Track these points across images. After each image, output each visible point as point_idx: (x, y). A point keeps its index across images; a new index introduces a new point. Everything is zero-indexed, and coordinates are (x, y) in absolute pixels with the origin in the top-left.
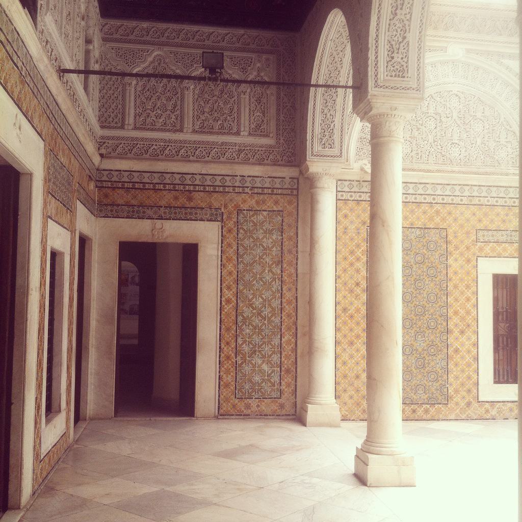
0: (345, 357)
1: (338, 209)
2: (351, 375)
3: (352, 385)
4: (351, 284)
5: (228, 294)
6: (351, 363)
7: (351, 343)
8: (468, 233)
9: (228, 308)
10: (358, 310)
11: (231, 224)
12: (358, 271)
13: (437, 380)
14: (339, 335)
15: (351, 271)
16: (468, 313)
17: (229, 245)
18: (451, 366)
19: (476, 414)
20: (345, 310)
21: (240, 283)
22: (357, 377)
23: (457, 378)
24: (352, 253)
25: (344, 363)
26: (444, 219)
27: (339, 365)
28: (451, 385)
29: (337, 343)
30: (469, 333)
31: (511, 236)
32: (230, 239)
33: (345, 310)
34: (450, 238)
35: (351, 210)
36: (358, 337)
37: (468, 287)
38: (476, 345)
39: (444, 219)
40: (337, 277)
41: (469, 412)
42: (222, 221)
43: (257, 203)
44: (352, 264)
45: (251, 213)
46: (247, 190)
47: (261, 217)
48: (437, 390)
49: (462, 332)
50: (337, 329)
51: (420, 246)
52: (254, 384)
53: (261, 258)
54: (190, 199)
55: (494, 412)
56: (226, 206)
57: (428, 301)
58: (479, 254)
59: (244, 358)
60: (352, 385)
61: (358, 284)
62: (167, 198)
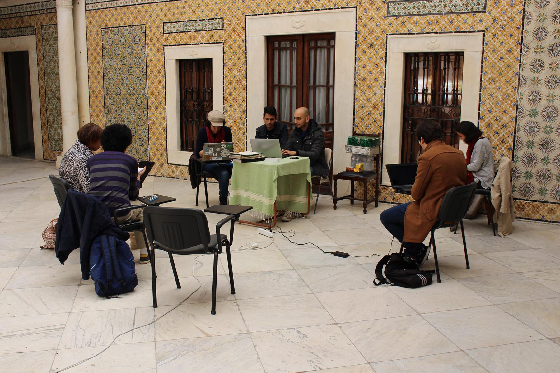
1: (86, 18)
5: (42, 84)
7: (97, 116)
8: (158, 26)
9: (42, 91)
10: (100, 92)
11: (39, 37)
12: (98, 63)
13: (142, 146)
14: (92, 110)
16: (160, 93)
17: (40, 50)
18: (151, 135)
19: (166, 173)
20: (93, 92)
21: (46, 75)
23: (154, 144)
24: (95, 49)
26: (143, 17)
28: (151, 149)
30: (161, 109)
31: (186, 26)
33: (93, 92)
34: (148, 32)
37: (159, 71)
38: (165, 119)
39: (143, 17)
40: (89, 68)
41: (163, 171)
42: (36, 34)
43: (49, 19)
44: (95, 58)
45: (47, 27)
46: (45, 11)
47: (51, 29)
48: (143, 152)
49: (156, 108)
50: (90, 106)
51: (130, 40)
52: (56, 141)
53: (53, 58)
54: (23, 22)
55: (178, 173)
56: (37, 24)
57: (136, 84)
58: (165, 44)
59: (50, 125)
61: (99, 73)
62: (14, 23)
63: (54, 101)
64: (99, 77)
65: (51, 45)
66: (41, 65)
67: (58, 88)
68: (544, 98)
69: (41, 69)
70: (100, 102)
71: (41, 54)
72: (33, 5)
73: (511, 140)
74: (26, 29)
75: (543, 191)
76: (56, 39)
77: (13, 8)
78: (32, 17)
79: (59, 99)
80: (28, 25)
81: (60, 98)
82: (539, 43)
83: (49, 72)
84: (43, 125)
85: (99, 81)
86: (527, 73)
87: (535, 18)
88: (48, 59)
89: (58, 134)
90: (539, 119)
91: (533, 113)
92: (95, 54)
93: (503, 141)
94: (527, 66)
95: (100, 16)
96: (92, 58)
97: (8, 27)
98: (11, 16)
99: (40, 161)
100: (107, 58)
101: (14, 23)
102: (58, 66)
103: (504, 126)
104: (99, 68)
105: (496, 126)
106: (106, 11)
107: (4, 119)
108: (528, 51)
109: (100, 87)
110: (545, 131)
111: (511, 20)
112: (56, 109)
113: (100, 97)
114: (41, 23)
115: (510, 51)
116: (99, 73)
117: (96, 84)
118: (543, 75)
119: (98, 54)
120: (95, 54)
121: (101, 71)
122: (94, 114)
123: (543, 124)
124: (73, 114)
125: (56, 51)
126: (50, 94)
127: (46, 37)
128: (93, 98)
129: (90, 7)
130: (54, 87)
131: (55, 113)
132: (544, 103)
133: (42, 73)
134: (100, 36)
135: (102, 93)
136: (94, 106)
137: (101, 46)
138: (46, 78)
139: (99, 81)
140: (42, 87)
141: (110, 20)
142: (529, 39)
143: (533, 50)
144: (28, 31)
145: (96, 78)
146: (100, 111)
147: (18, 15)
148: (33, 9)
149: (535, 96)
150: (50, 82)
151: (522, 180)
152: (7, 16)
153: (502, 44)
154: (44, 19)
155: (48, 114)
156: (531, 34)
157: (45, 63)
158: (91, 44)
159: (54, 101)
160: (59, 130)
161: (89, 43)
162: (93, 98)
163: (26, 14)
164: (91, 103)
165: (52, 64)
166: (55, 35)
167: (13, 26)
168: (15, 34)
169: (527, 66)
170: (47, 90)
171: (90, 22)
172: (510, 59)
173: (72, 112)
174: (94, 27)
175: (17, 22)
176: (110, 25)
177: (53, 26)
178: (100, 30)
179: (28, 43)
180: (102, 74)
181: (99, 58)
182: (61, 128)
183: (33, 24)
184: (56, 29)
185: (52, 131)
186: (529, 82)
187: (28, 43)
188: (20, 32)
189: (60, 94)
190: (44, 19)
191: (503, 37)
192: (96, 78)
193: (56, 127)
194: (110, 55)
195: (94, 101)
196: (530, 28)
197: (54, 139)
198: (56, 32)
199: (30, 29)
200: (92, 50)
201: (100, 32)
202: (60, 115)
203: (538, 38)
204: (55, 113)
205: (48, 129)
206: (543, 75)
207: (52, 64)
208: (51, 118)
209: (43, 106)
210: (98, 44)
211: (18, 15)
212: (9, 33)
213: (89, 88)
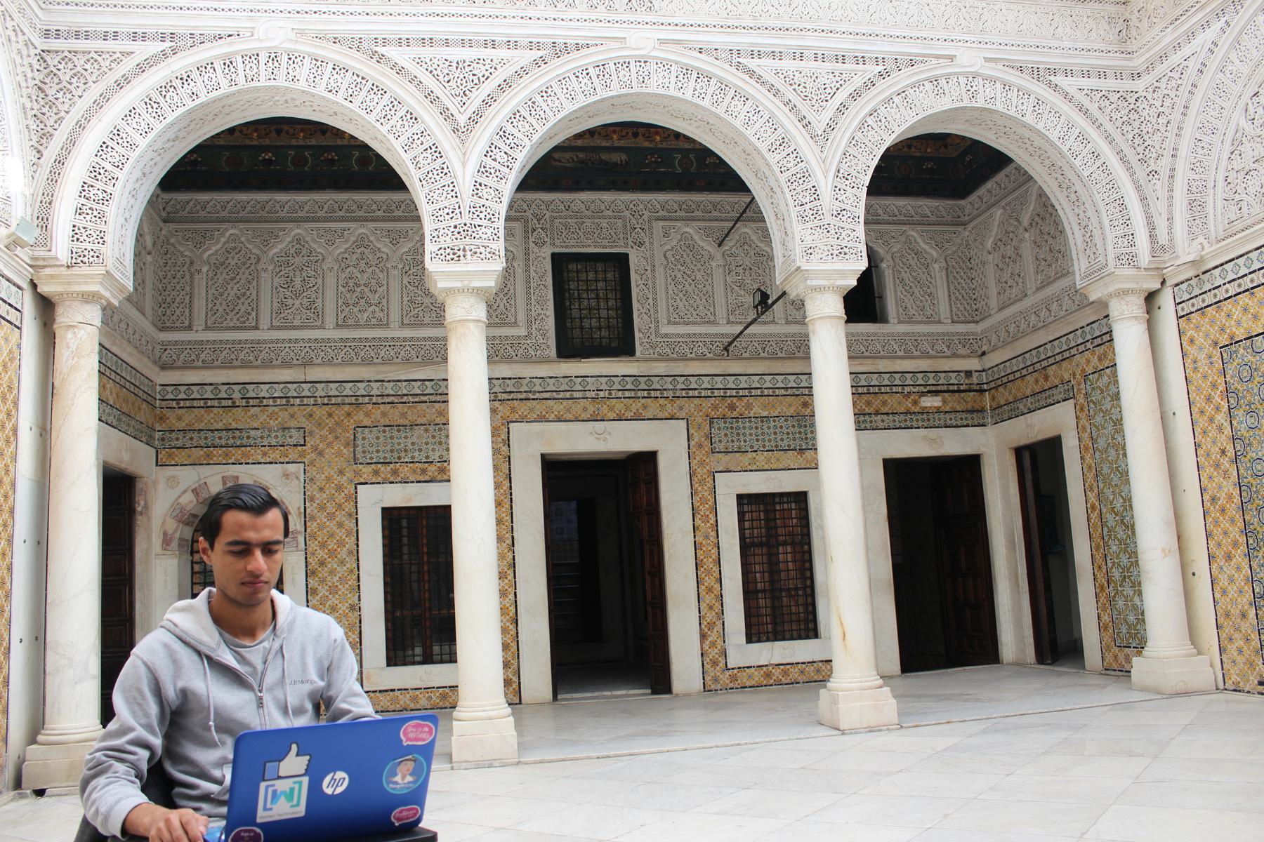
0: (1223, 581)
2: (1235, 612)
3: (1238, 629)
4: (1215, 454)
6: (1232, 591)
7: (1229, 557)
9: (1094, 516)
10: (1230, 497)
11: (1081, 400)
15: (1213, 432)
17: (1084, 428)
20: (1214, 499)
22: (1244, 616)
24: (1209, 399)
25: (1224, 592)
27: (1218, 596)
29: (1211, 558)
32: (1084, 422)
33: (1214, 499)
35: (1197, 328)
36: (1236, 544)
40: (1197, 446)
42: (1074, 397)
43: (1100, 359)
44: (1211, 420)
45: (1096, 375)
46: (1089, 345)
50: (1208, 535)
53: (1113, 438)
54: (1046, 378)
56: (1074, 375)
60: (1238, 629)
61: (1223, 452)
62: (1030, 385)
63: (1121, 533)
64: (1225, 463)
65: (1106, 412)
66: (1088, 460)
67: (1128, 502)
69: (1090, 468)
70: (1233, 521)
71: (1086, 436)
72: (1063, 339)
74: (1054, 391)
76: (1117, 396)
77: (1027, 355)
78: (1064, 364)
79: (1130, 527)
80: (1057, 382)
81: (1133, 526)
83: (1105, 470)
84: (1099, 590)
85: (1225, 472)
88: (1101, 443)
89: (1135, 608)
92: (1210, 410)
95: (1212, 322)
96: (1202, 422)
97: (1020, 395)
98: (1024, 372)
99: (1093, 672)
100: (1241, 413)
101: (1030, 385)
102: (1125, 455)
104: (1224, 440)
106: (1227, 306)
107: (1018, 586)
109: (1229, 487)
112: (1125, 551)
113: (1233, 510)
114: (1083, 371)
116: (1223, 452)
117: (1218, 479)
119: (1218, 409)
120: (1210, 410)
121: (1230, 448)
122: (1219, 554)
124: (1166, 556)
125: (1118, 423)
126: (1111, 520)
127: (1096, 396)
128: (1215, 513)
129: (1187, 307)
130: (1118, 504)
131: (1124, 560)
133: (1090, 476)
134: (1218, 365)
135: (1237, 499)
136: (1217, 533)
137: (1222, 387)
138: (1101, 485)
139: (1225, 472)
140: (1093, 507)
141: (1239, 323)
144: (1058, 394)
145: (1217, 466)
146: (1236, 544)
147: (1038, 366)
148: (1065, 347)
150: (1108, 492)
152: (1017, 375)
154: (1088, 361)
155: (1110, 565)
157: (1098, 453)
158: (1199, 389)
159: (1121, 533)
160: (1136, 599)
161: (1192, 388)
162: (1215, 513)
163: (1051, 361)
164: (1210, 527)
165: (1112, 452)
166: (1113, 389)
167: (1028, 392)
168: (1032, 407)
170: (1104, 510)
171: (1192, 341)
173: (1163, 550)
174: (1200, 349)
175: (1037, 381)
176: (1240, 334)
177: (1108, 371)
178: (1217, 353)
179: (1059, 420)
180: (1231, 453)
181: (1221, 418)
182: (1140, 593)
183: (1066, 377)
184: (1115, 375)
185: (1121, 603)
187: (1059, 420)
188: (1043, 399)
189: (1132, 517)
190: (1088, 361)
192: (1217, 466)
193: (1129, 591)
194: (1250, 404)
195: (1216, 523)
197: (1125, 620)
198: (1116, 382)
199: (1061, 389)
200: (1200, 402)
201: (1217, 358)
202: (1137, 564)
204: (1124, 560)
205: (1111, 599)
207: (1112, 452)
208: (1116, 573)
209: (1098, 548)
210: (1214, 386)
211: (1038, 366)
212: (1021, 407)
213: (1202, 491)
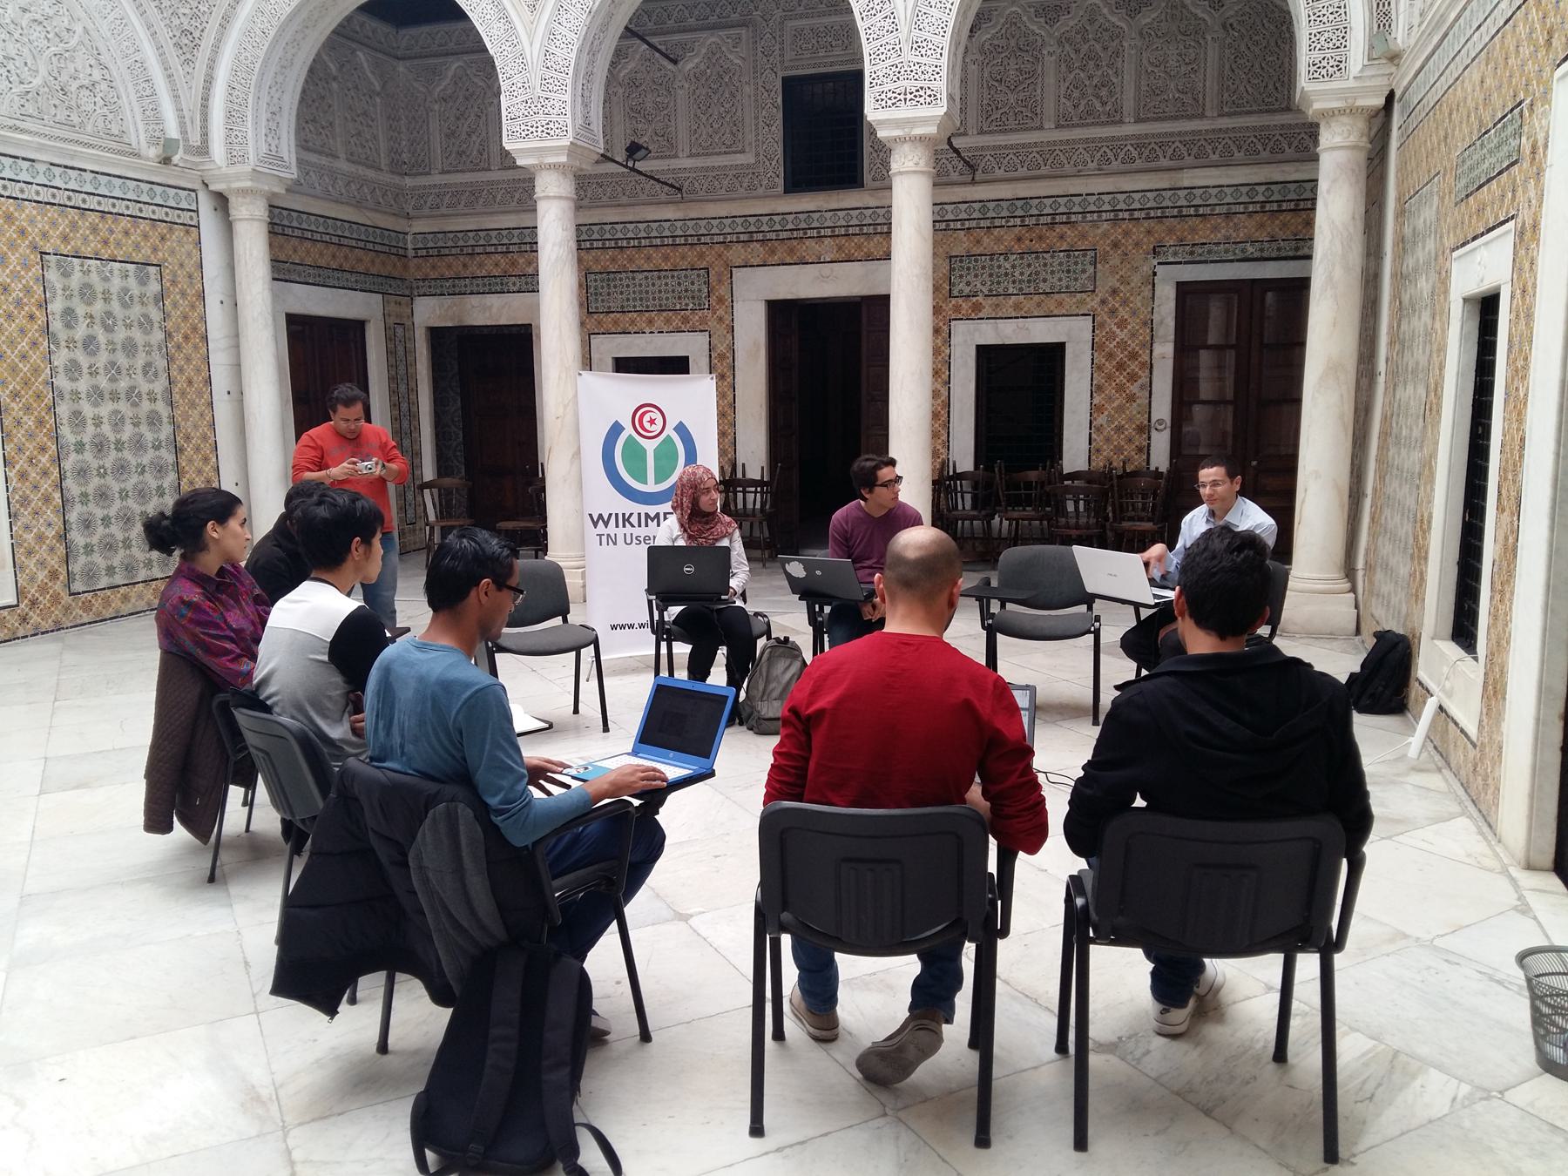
68: (90, 422)
73: (57, 495)
75: (110, 570)
82: (71, 333)
86: (62, 382)
87: (60, 292)
90: (88, 456)
91: (80, 448)
93: (47, 499)
94: (61, 370)
103: (45, 473)
105: (33, 475)
108: (58, 345)
110: (99, 474)
111: (28, 291)
115: (34, 344)
118: (83, 385)
123: (95, 464)
132: (90, 429)
142: (57, 326)
143: (63, 344)
149: (77, 419)
151: (82, 559)
153: (22, 331)
156: (58, 317)
169: (61, 370)
172: (35, 357)
186: (67, 397)
191: (20, 320)
196: (56, 306)
203: (68, 326)
206: (83, 385)
